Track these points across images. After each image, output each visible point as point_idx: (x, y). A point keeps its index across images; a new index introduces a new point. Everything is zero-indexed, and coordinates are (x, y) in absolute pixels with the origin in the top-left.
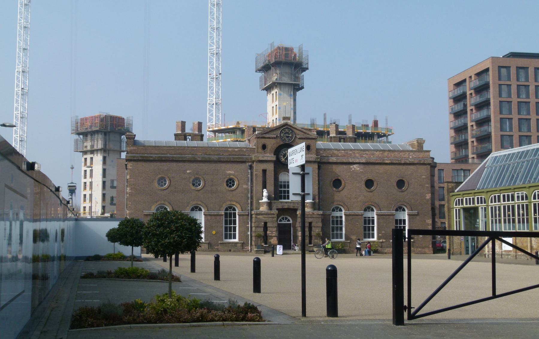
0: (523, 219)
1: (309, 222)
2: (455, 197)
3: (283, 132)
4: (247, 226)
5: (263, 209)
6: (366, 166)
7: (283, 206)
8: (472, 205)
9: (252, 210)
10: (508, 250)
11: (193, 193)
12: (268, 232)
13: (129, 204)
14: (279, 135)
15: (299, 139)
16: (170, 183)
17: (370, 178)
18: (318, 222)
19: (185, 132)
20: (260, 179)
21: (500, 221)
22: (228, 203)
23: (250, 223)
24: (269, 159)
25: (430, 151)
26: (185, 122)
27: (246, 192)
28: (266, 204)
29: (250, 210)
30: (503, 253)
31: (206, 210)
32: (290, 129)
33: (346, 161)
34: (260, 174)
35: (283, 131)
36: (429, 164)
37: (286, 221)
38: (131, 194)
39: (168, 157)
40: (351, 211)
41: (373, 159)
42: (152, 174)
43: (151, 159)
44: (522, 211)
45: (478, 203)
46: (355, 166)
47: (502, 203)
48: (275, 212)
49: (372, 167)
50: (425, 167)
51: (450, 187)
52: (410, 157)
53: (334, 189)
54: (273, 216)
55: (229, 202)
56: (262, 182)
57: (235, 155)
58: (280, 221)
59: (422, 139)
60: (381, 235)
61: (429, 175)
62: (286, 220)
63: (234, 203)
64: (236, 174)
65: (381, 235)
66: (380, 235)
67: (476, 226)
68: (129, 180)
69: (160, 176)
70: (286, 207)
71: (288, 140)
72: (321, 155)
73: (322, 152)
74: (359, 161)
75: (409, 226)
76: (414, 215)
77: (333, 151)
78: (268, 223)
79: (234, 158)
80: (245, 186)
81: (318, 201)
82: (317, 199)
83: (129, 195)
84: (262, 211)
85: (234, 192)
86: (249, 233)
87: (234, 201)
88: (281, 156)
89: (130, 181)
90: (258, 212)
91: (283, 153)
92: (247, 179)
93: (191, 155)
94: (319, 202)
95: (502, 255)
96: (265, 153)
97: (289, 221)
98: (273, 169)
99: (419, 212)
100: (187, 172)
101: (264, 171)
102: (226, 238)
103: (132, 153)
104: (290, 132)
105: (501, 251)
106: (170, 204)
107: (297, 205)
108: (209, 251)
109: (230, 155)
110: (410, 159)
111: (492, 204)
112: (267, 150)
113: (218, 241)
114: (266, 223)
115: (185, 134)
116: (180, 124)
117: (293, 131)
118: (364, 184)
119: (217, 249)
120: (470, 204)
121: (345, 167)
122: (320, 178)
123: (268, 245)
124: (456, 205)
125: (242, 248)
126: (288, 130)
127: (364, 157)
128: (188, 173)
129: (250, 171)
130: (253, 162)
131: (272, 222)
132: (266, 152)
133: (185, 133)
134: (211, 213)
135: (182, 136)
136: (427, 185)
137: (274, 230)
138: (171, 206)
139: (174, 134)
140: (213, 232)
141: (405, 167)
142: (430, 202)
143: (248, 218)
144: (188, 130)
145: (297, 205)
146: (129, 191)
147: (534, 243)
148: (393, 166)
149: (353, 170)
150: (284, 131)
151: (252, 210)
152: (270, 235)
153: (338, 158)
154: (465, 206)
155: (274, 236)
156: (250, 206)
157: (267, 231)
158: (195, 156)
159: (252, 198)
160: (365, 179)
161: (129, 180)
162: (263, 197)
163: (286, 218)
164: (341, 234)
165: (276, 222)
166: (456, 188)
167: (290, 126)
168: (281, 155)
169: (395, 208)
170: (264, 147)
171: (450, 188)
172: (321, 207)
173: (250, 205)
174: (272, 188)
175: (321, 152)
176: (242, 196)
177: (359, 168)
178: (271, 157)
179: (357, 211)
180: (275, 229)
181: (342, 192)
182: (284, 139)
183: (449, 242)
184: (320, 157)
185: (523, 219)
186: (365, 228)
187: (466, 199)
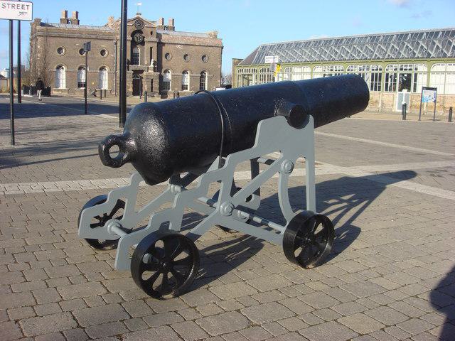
46: (179, 46)
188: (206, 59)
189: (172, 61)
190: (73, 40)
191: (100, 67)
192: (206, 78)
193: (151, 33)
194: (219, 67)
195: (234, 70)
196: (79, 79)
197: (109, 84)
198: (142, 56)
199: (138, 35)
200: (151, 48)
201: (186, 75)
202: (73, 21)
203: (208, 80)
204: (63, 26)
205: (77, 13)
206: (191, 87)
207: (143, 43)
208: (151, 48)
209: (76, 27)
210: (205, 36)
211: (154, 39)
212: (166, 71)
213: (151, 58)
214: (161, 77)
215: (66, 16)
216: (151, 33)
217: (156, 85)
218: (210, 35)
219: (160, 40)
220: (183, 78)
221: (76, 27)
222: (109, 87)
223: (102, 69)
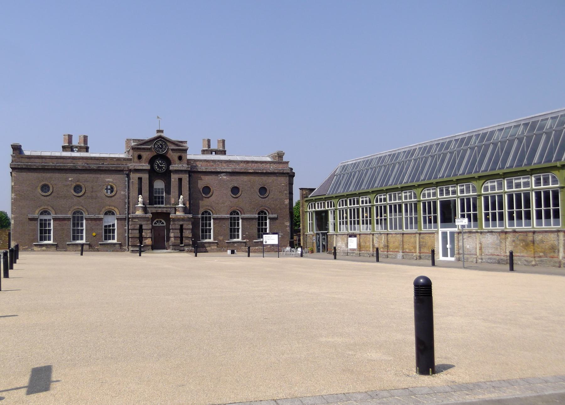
0: (367, 221)
3: (157, 144)
4: (125, 228)
5: (139, 213)
7: (157, 210)
8: (323, 209)
9: (128, 214)
10: (353, 249)
11: (75, 199)
12: (143, 234)
13: (14, 209)
16: (53, 189)
17: (235, 186)
18: (189, 224)
19: (72, 144)
20: (136, 186)
21: (346, 222)
22: (107, 208)
23: (127, 225)
24: (144, 168)
25: (288, 162)
26: (72, 135)
27: (123, 198)
29: (127, 215)
30: (349, 251)
33: (214, 170)
34: (136, 181)
35: (157, 143)
37: (160, 224)
39: (51, 166)
43: (35, 167)
44: (366, 213)
45: (328, 207)
47: (349, 206)
48: (149, 215)
51: (304, 193)
53: (204, 195)
55: (108, 207)
56: (138, 188)
57: (114, 165)
58: (155, 223)
60: (245, 236)
61: (288, 183)
63: (113, 208)
65: (245, 236)
66: (244, 236)
67: (326, 227)
69: (44, 183)
72: (191, 165)
74: (226, 171)
75: (270, 228)
78: (143, 226)
79: (112, 167)
80: (122, 193)
81: (188, 205)
82: (188, 204)
83: (14, 200)
85: (113, 198)
86: (127, 235)
88: (156, 166)
90: (134, 215)
92: (124, 186)
93: (72, 164)
94: (190, 206)
95: (347, 253)
96: (140, 163)
97: (163, 223)
100: (69, 179)
101: (140, 179)
102: (106, 239)
104: (164, 144)
105: (347, 249)
106: (53, 209)
108: (90, 251)
110: (271, 169)
111: (340, 207)
112: (142, 160)
114: (141, 226)
115: (71, 146)
116: (67, 137)
118: (230, 191)
119: (97, 249)
120: (321, 208)
122: (191, 185)
125: (120, 248)
127: (230, 167)
128: (70, 180)
129: (127, 179)
132: (141, 162)
133: (71, 145)
135: (69, 147)
136: (286, 192)
137: (148, 232)
138: (53, 210)
139: (62, 146)
142: (288, 207)
144: (75, 142)
147: (376, 242)
149: (220, 178)
150: (158, 142)
151: (128, 214)
152: (145, 236)
153: (207, 167)
154: (317, 209)
155: (149, 238)
157: (142, 233)
158: (77, 165)
159: (129, 203)
160: (231, 186)
161: (13, 186)
163: (161, 221)
164: (210, 236)
165: (151, 225)
168: (156, 164)
169: (257, 212)
170: (140, 157)
171: (305, 194)
172: (191, 212)
176: (120, 202)
177: (225, 177)
178: (147, 166)
182: (158, 150)
184: (190, 166)
185: (367, 221)
186: (231, 229)
193: (180, 158)
200: (180, 180)
216: (180, 158)
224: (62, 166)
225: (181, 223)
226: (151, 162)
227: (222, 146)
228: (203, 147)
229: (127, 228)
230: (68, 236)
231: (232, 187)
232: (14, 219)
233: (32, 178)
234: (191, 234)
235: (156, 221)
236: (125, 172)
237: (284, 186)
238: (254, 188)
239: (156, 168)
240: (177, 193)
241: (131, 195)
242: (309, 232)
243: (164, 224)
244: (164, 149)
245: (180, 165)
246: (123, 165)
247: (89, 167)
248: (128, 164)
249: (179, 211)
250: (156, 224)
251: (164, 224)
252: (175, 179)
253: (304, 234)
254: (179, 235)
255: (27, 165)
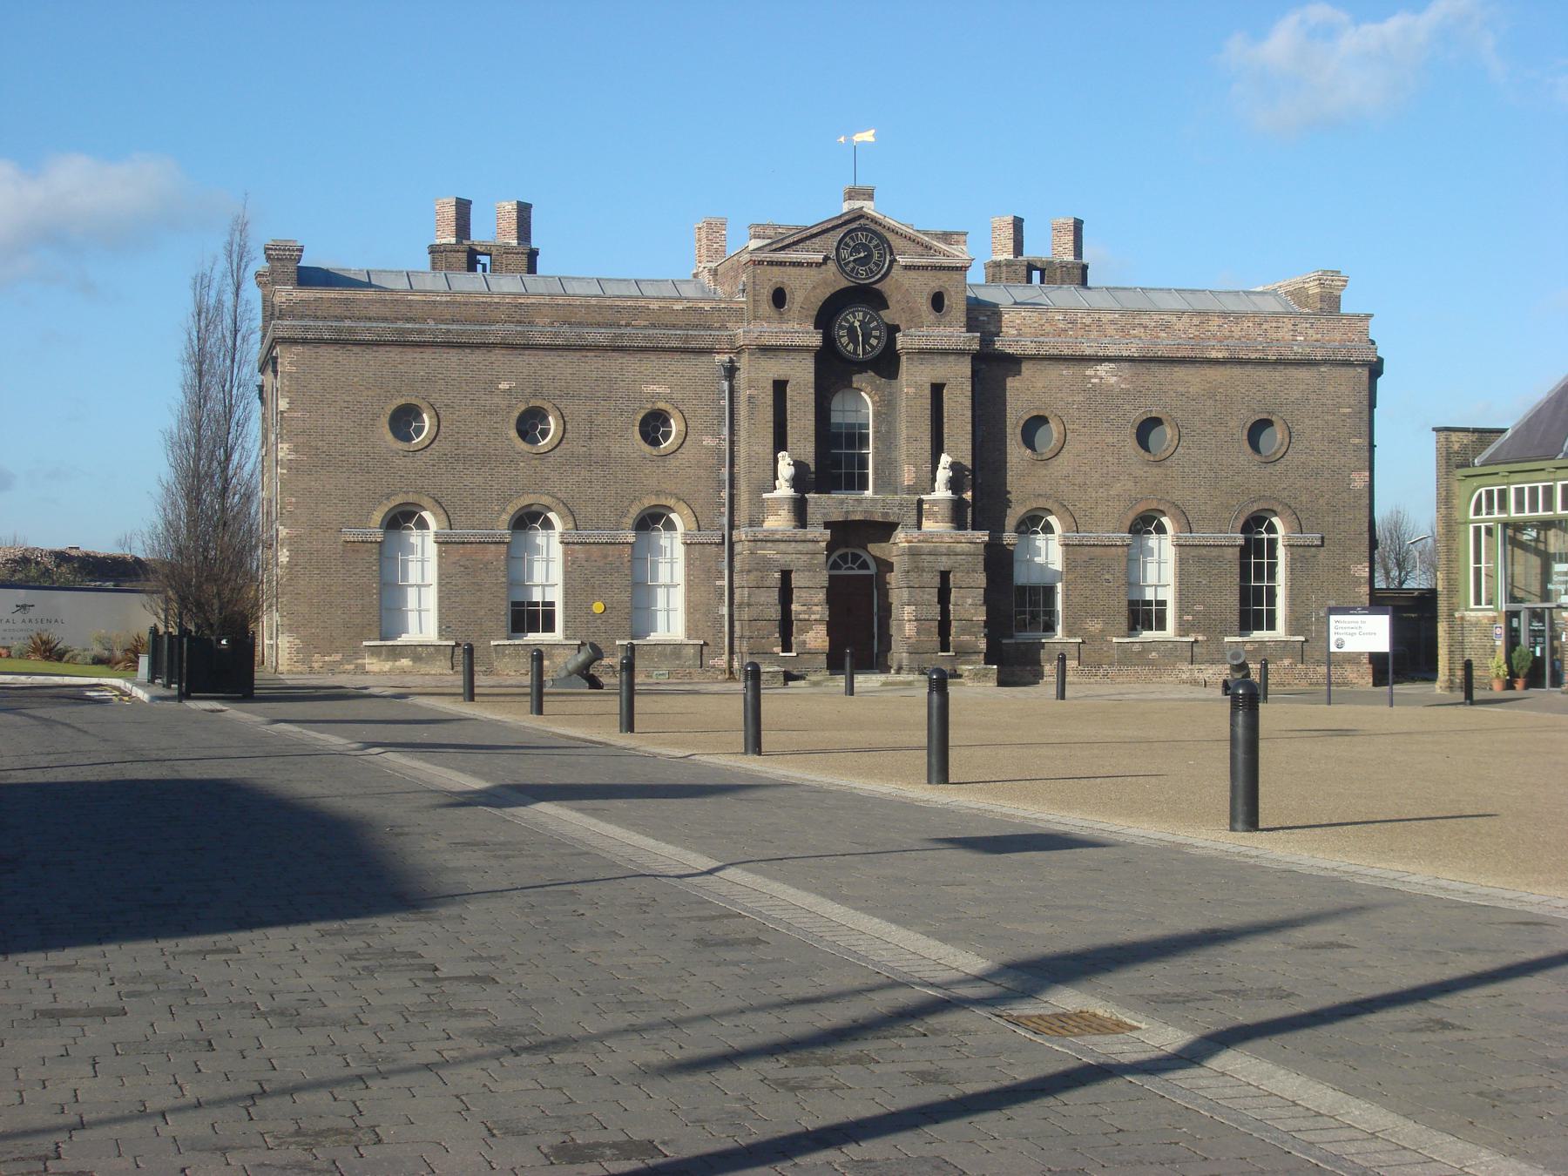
1: (942, 572)
2: (1475, 482)
3: (847, 245)
4: (718, 583)
5: (779, 522)
6: (1141, 368)
11: (522, 464)
12: (794, 607)
14: (833, 255)
15: (907, 267)
17: (1154, 415)
22: (651, 501)
23: (726, 572)
24: (798, 342)
25: (1371, 316)
28: (786, 507)
29: (726, 528)
31: (571, 525)
32: (874, 232)
36: (1364, 364)
37: (854, 569)
38: (291, 466)
39: (433, 332)
40: (1085, 531)
41: (1165, 345)
42: (370, 393)
43: (368, 337)
46: (1102, 369)
48: (819, 534)
49: (1162, 373)
50: (1351, 372)
52: (1298, 338)
54: (810, 546)
57: (674, 327)
59: (1339, 272)
62: (853, 562)
63: (671, 502)
64: (677, 395)
68: (285, 415)
70: (858, 517)
71: (867, 274)
73: (985, 318)
76: (1309, 546)
77: (1023, 314)
78: (793, 575)
80: (708, 441)
84: (774, 532)
85: (673, 463)
86: (725, 610)
87: (671, 494)
89: (292, 419)
91: (848, 321)
92: (716, 413)
96: (782, 320)
98: (811, 377)
99: (1327, 537)
100: (500, 386)
101: (780, 387)
103: (294, 317)
107: (896, 509)
109: (654, 326)
110: (1298, 345)
113: (614, 639)
114: (786, 575)
117: (883, 240)
118: (1134, 436)
121: (1066, 371)
123: (795, 654)
124: (1478, 511)
126: (867, 236)
128: (504, 391)
129: (726, 384)
130: (739, 351)
131: (810, 568)
134: (588, 536)
136: (1357, 441)
140: (595, 605)
141: (1279, 374)
143: (719, 555)
145: (896, 509)
146: (289, 457)
148: (1237, 371)
150: (852, 238)
151: (732, 527)
152: (802, 617)
154: (1513, 513)
156: (727, 513)
162: (777, 482)
166: (1476, 453)
167: (874, 220)
168: (841, 327)
170: (779, 298)
173: (726, 510)
174: (807, 451)
175: (981, 318)
179: (1108, 532)
180: (821, 596)
181: (1055, 462)
183: (1450, 646)
187: (1520, 492)
188: (1274, 439)
189: (1064, 463)
190: (476, 357)
191: (635, 511)
192: (1281, 552)
193: (938, 301)
194: (1359, 480)
195: (1446, 500)
196: (516, 579)
197: (691, 609)
198: (887, 439)
199: (856, 318)
200: (937, 390)
201: (1153, 541)
202: (500, 259)
203: (1292, 569)
204: (435, 282)
205: (524, 211)
206: (1182, 610)
207: (886, 363)
208: (937, 390)
209: (508, 284)
210: (1271, 305)
211: (954, 334)
212: (1033, 523)
213: (937, 449)
214: (998, 562)
215: (463, 228)
216: (938, 301)
217: (969, 606)
218: (1299, 295)
219: (987, 340)
220: (1133, 560)
221: (508, 284)
222: (691, 630)
223: (651, 520)
224: (412, 331)
225: (944, 563)
226: (826, 316)
227: (1070, 246)
228: (994, 252)
229: (726, 583)
230: (497, 614)
231: (1138, 422)
232: (290, 544)
233: (355, 379)
234: (985, 608)
235: (839, 557)
236: (718, 357)
237: (1349, 415)
238: (1231, 424)
239: (845, 340)
240: (927, 445)
241: (742, 450)
242: (1472, 605)
243: (868, 568)
244: (878, 265)
245: (941, 330)
246: (709, 328)
247: (580, 336)
248: (728, 325)
249: (933, 516)
250: (839, 567)
251: (868, 568)
252: (918, 386)
253: (1451, 615)
254: (936, 611)
255: (339, 330)
